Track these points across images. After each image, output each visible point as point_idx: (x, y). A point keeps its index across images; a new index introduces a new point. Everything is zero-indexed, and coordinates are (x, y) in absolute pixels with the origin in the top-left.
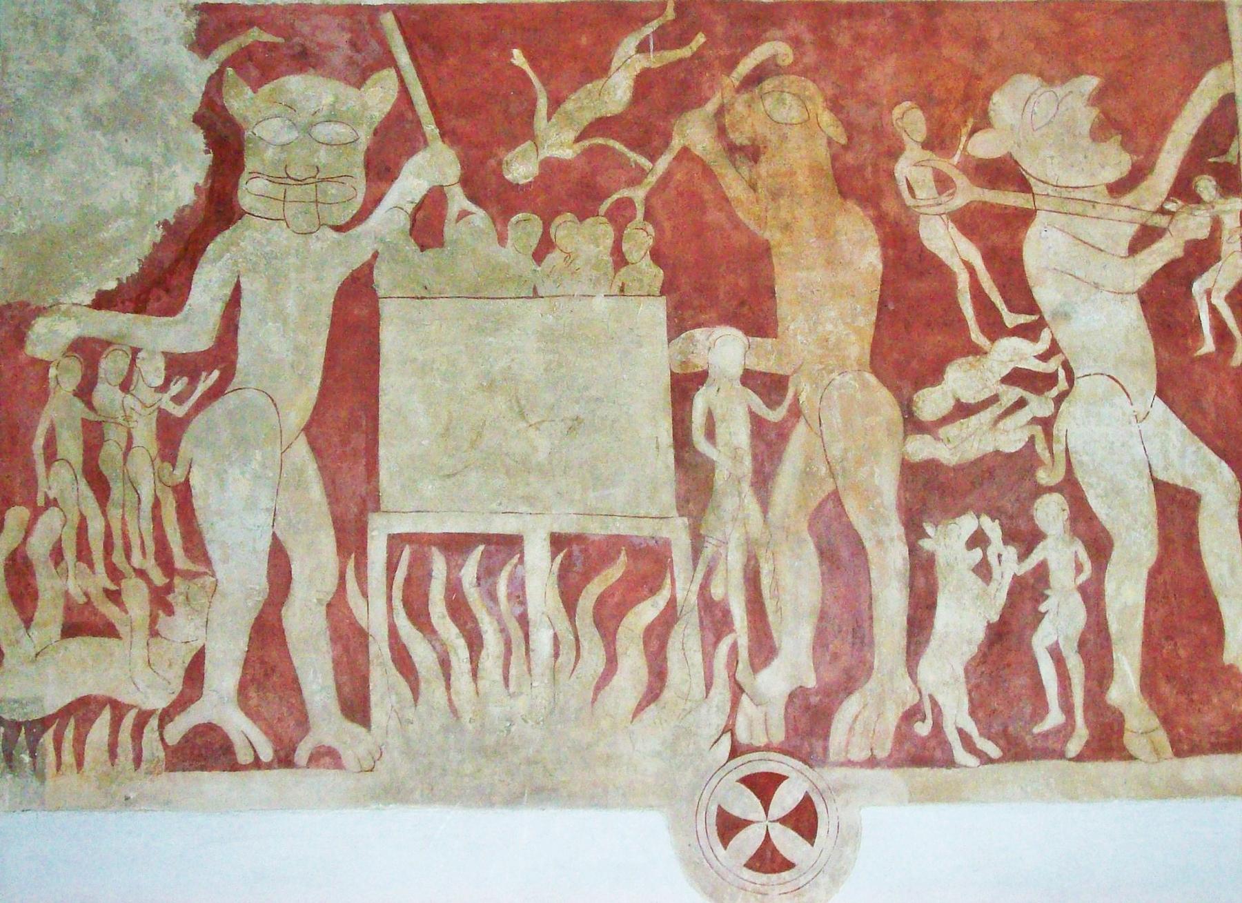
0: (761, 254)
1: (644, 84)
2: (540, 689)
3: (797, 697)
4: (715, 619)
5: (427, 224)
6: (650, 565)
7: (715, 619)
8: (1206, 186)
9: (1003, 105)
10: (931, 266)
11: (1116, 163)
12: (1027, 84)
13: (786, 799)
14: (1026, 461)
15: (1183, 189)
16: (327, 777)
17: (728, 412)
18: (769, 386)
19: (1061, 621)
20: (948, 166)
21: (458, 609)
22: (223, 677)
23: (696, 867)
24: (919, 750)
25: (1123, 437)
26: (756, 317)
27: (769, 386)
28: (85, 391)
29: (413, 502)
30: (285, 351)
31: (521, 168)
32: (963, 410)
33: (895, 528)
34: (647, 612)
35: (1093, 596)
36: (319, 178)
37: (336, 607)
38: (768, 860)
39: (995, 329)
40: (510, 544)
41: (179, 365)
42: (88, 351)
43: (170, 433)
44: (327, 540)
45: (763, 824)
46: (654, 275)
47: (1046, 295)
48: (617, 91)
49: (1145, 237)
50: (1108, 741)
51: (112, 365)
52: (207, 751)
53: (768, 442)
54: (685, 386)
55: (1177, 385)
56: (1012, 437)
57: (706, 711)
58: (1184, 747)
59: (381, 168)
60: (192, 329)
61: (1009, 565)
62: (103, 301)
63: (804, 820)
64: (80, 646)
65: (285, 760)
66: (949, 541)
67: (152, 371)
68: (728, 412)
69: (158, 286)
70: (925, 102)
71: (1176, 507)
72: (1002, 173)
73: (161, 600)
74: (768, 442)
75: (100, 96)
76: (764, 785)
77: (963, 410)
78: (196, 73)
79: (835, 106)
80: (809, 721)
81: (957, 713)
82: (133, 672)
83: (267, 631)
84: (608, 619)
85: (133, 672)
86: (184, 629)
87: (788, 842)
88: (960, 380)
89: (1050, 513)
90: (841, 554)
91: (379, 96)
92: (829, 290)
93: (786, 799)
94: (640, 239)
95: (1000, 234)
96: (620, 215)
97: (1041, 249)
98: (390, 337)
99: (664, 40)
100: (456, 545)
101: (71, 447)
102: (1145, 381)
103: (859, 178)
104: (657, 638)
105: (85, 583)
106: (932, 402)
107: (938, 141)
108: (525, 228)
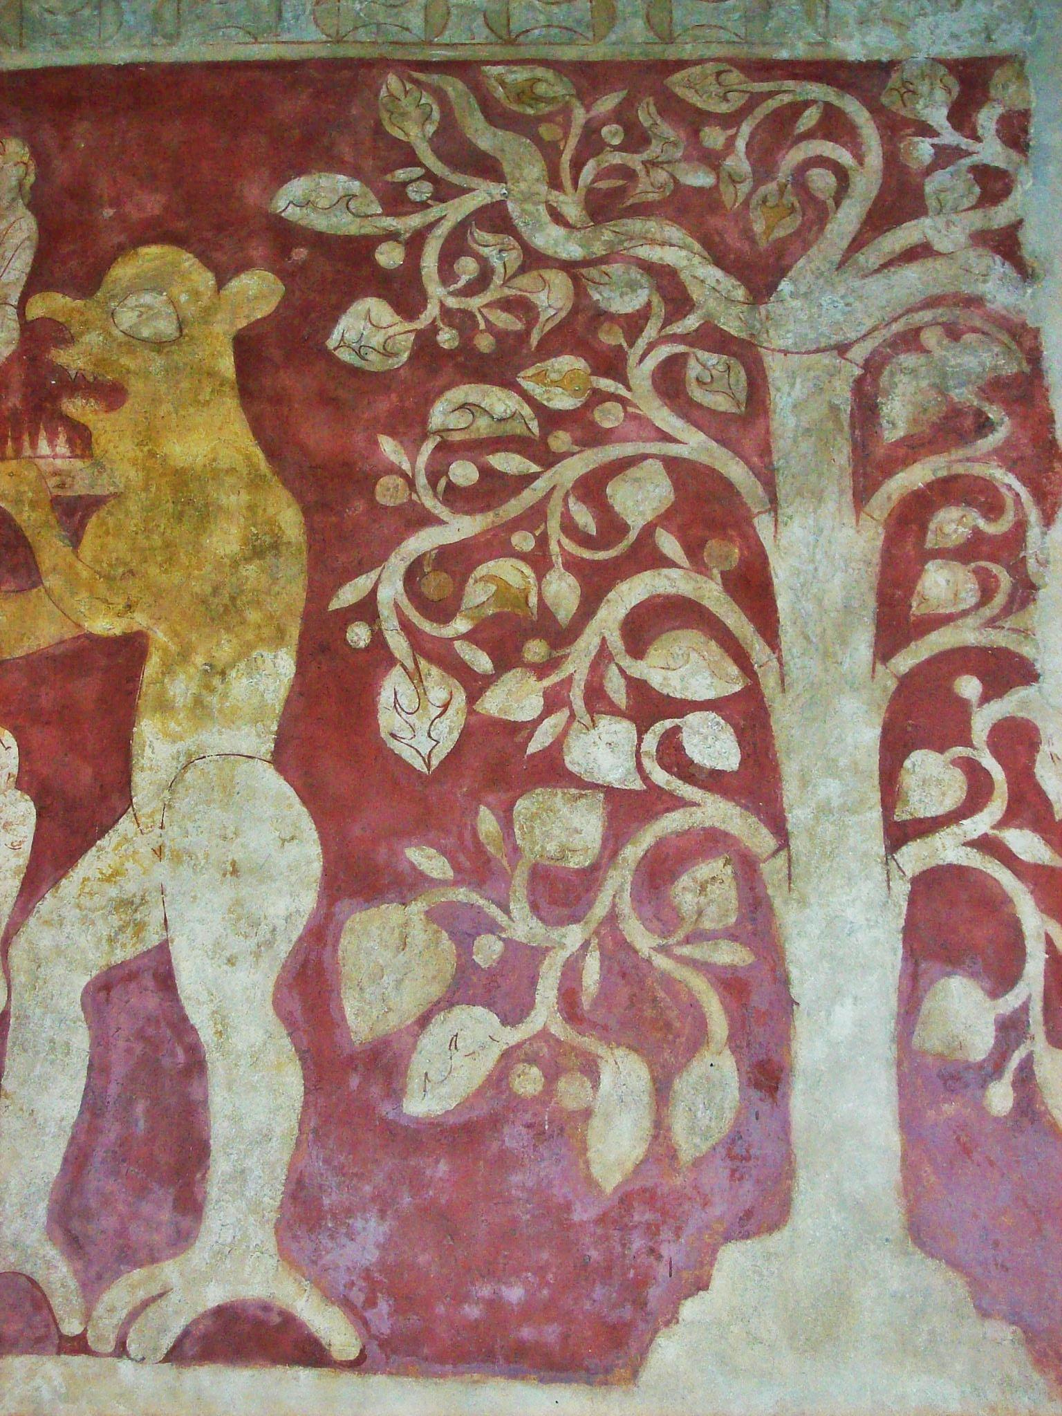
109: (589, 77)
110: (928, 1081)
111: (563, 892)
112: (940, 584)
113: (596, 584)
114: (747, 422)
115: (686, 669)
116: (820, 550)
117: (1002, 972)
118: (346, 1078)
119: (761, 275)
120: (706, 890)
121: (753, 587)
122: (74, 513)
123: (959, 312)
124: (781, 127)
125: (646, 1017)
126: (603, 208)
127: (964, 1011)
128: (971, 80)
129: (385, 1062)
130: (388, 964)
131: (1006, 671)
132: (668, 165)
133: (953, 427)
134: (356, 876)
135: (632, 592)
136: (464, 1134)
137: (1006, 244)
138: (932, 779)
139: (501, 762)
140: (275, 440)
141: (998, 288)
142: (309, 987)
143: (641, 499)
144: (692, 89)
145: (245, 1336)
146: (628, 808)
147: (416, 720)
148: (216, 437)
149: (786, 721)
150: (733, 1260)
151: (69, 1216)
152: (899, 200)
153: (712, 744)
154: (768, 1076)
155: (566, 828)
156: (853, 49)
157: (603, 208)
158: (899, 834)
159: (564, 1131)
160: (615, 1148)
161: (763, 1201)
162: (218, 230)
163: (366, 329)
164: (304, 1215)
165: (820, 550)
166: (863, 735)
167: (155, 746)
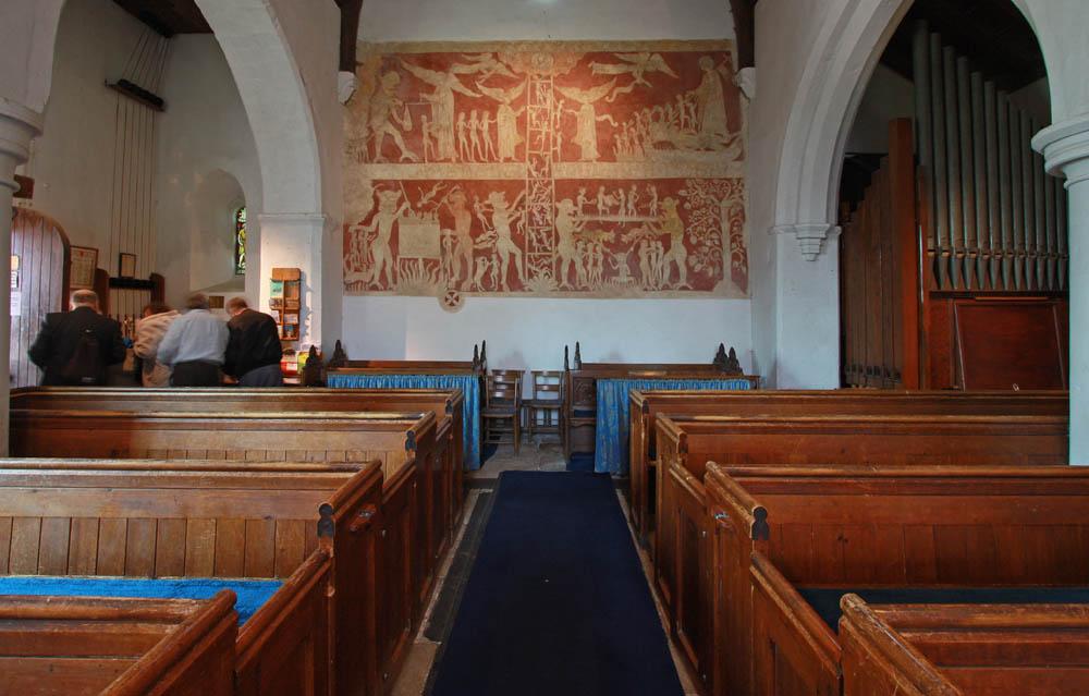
0: (453, 218)
1: (438, 192)
2: (420, 281)
3: (457, 282)
4: (446, 271)
5: (406, 213)
6: (436, 263)
7: (446, 271)
8: (520, 209)
9: (490, 196)
10: (478, 220)
11: (507, 205)
12: (494, 193)
13: (455, 296)
14: (491, 249)
15: (516, 209)
16: (390, 292)
17: (448, 242)
18: (454, 237)
19: (495, 272)
20: (482, 205)
21: (409, 267)
22: (377, 278)
23: (441, 304)
24: (474, 289)
25: (505, 245)
26: (453, 227)
27: (454, 237)
28: (357, 237)
29: (403, 253)
30: (385, 231)
31: (419, 205)
32: (482, 241)
33: (471, 258)
34: (436, 269)
35: (500, 269)
36: (390, 206)
37: (393, 268)
38: (452, 304)
39: (488, 230)
40: (417, 260)
41: (370, 233)
42: (358, 231)
43: (369, 243)
44: (391, 261)
45: (451, 299)
46: (437, 221)
47: (495, 224)
48: (434, 193)
49: (510, 216)
50: (500, 289)
51: (361, 233)
52: (374, 288)
53: (454, 245)
54: (442, 237)
55: (514, 238)
56: (489, 245)
57: (447, 283)
58: (511, 290)
59: (399, 205)
60: (372, 228)
61: (488, 264)
62: (360, 224)
63: (457, 299)
64: (358, 273)
65: (385, 289)
66: (479, 260)
67: (367, 234)
68: (448, 242)
69: (367, 222)
70: (478, 195)
71: (512, 256)
72: (489, 206)
73: (368, 267)
74: (454, 245)
75: (358, 193)
76: (452, 294)
77: (482, 241)
78: (372, 190)
79: (466, 196)
80: (458, 286)
81: (479, 284)
82: (364, 276)
83: (383, 272)
84: (430, 271)
85: (364, 276)
86: (371, 271)
87: (455, 302)
88: (482, 237)
89: (494, 257)
90: (463, 261)
91: (399, 194)
92: (463, 224)
93: (455, 296)
94: (436, 215)
95: (489, 215)
96: (434, 212)
97: (495, 217)
98: (400, 230)
99: (441, 185)
100: (409, 260)
101: (355, 245)
102: (509, 237)
103: (469, 207)
104: (437, 273)
105: (357, 264)
106: (478, 240)
107: (480, 202)
108: (420, 214)
109: (705, 180)
110: (734, 270)
111: (706, 255)
112: (735, 229)
113: (707, 228)
114: (719, 214)
115: (714, 236)
116: (725, 226)
117: (739, 259)
118: (690, 269)
119: (720, 200)
120: (717, 254)
121: (720, 229)
122: (664, 222)
123: (737, 204)
124: (722, 185)
125: (712, 264)
126: (707, 193)
127: (736, 263)
128: (739, 180)
129: (693, 268)
130: (693, 260)
131: (740, 236)
132: (712, 190)
133: (737, 215)
134: (690, 253)
135: (710, 230)
136: (699, 273)
137: (741, 197)
138: (734, 245)
139: (700, 244)
140: (680, 217)
141: (740, 201)
142: (687, 263)
143: (711, 221)
144: (716, 182)
145: (684, 288)
146: (710, 248)
147: (693, 240)
148: (675, 215)
149: (723, 241)
150: (720, 283)
151: (670, 280)
152: (732, 192)
153: (717, 243)
154: (722, 269)
155: (706, 250)
156: (729, 176)
157: (707, 193)
158: (731, 249)
159: (706, 273)
160: (710, 274)
161: (722, 279)
162: (675, 196)
163: (687, 206)
164: (688, 279)
165: (725, 226)
166: (728, 241)
167: (673, 243)
